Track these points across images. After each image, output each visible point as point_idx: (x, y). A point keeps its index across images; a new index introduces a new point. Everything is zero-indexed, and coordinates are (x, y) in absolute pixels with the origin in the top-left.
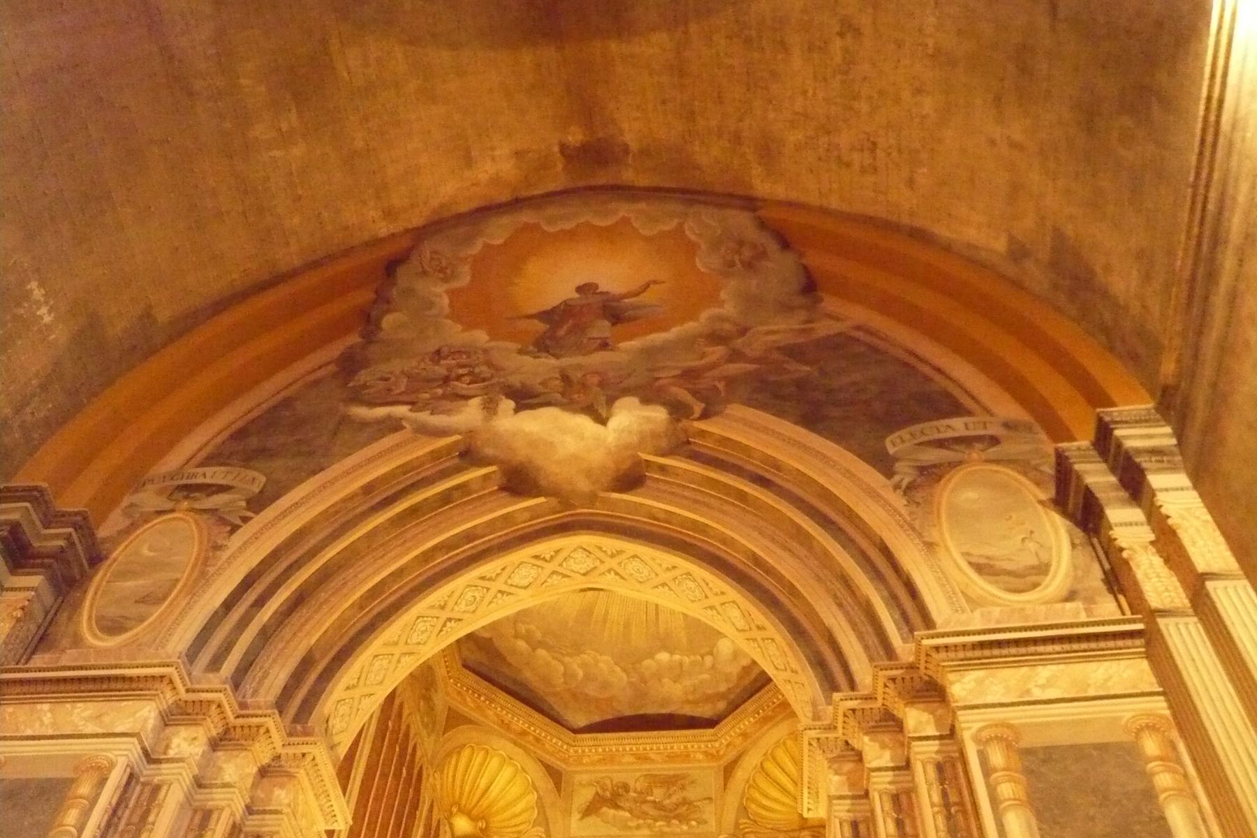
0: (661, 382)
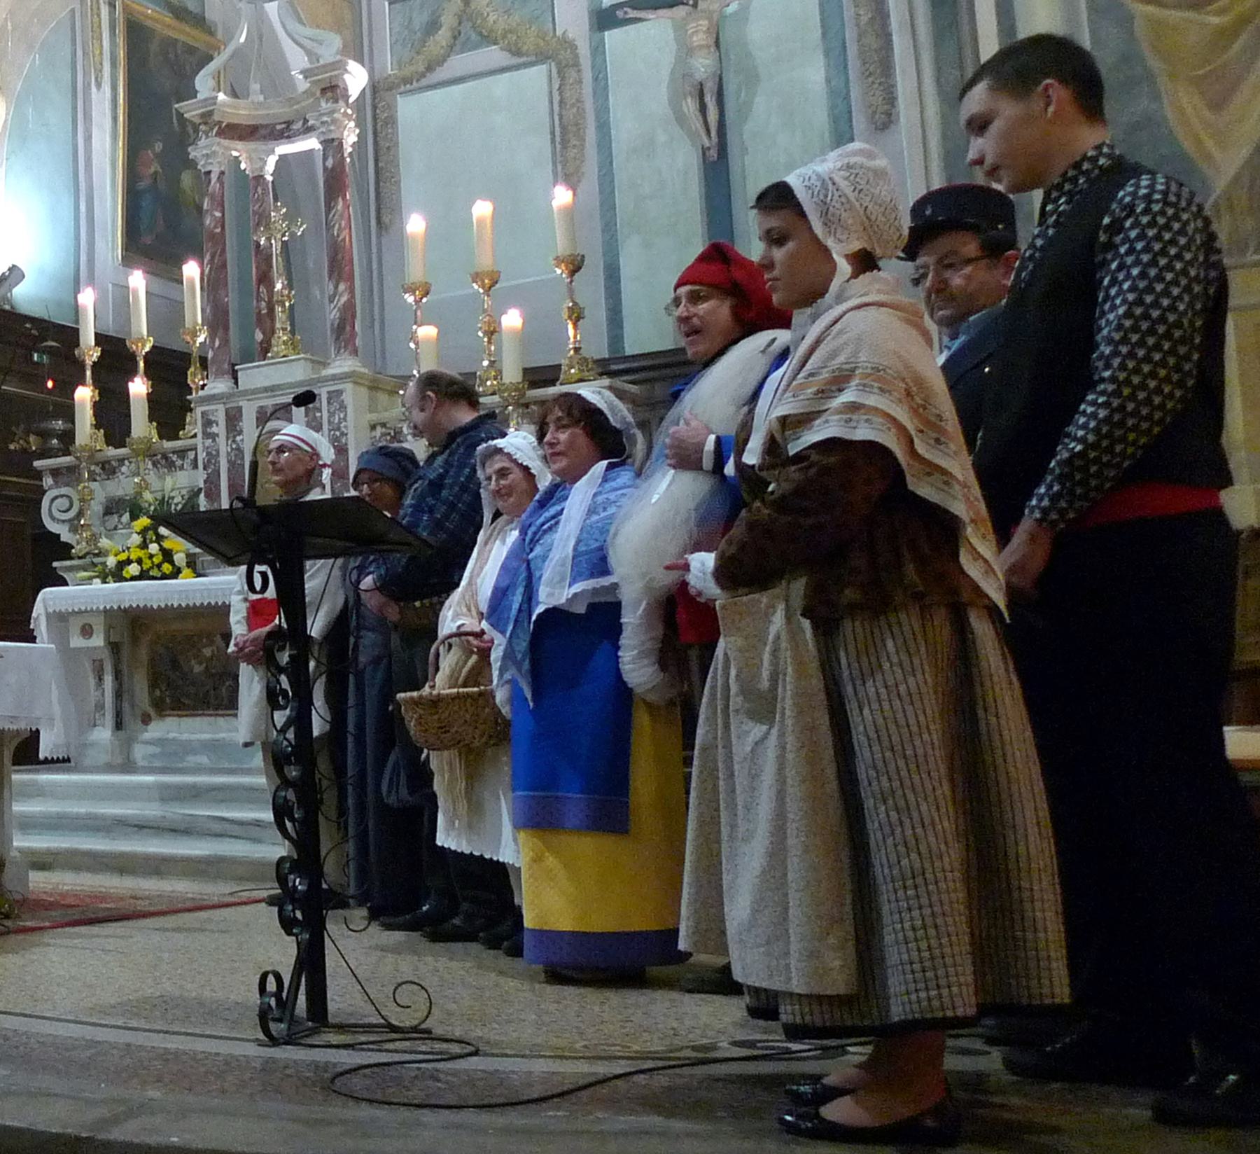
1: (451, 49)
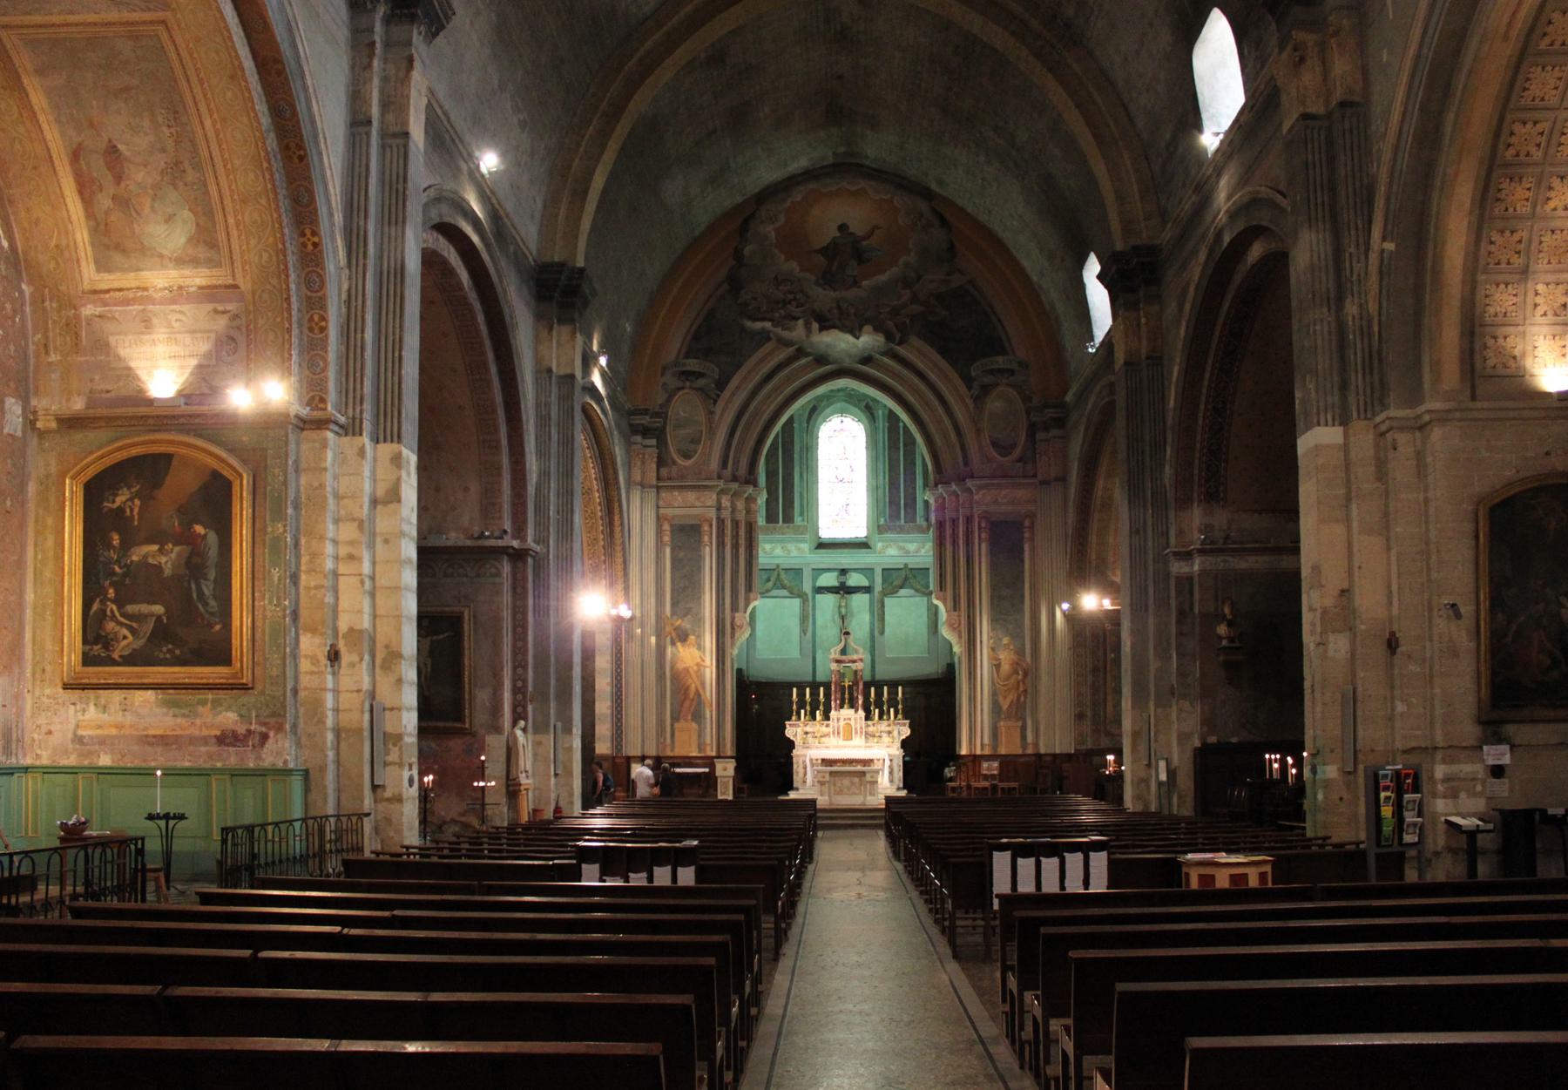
0: (882, 316)
1: (772, 588)
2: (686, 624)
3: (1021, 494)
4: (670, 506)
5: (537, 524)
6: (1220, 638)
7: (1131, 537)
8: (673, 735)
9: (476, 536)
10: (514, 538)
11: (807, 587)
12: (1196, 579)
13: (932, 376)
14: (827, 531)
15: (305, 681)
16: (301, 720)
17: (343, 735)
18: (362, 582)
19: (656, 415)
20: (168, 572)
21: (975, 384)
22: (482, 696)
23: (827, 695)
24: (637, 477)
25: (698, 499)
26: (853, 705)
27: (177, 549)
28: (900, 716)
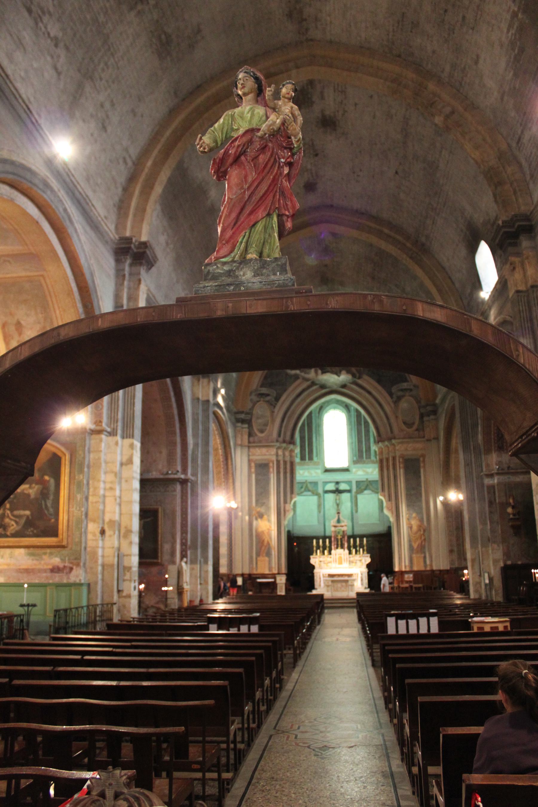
2: (262, 510)
3: (419, 446)
4: (254, 455)
5: (193, 467)
6: (509, 514)
7: (465, 467)
8: (257, 563)
9: (165, 473)
10: (182, 474)
11: (320, 491)
12: (496, 487)
13: (374, 393)
14: (329, 465)
15: (90, 543)
16: (88, 561)
17: (105, 567)
18: (116, 499)
19: (247, 413)
20: (33, 496)
21: (394, 396)
22: (167, 547)
23: (330, 542)
24: (239, 442)
25: (267, 451)
26: (342, 547)
27: (37, 487)
28: (365, 552)
